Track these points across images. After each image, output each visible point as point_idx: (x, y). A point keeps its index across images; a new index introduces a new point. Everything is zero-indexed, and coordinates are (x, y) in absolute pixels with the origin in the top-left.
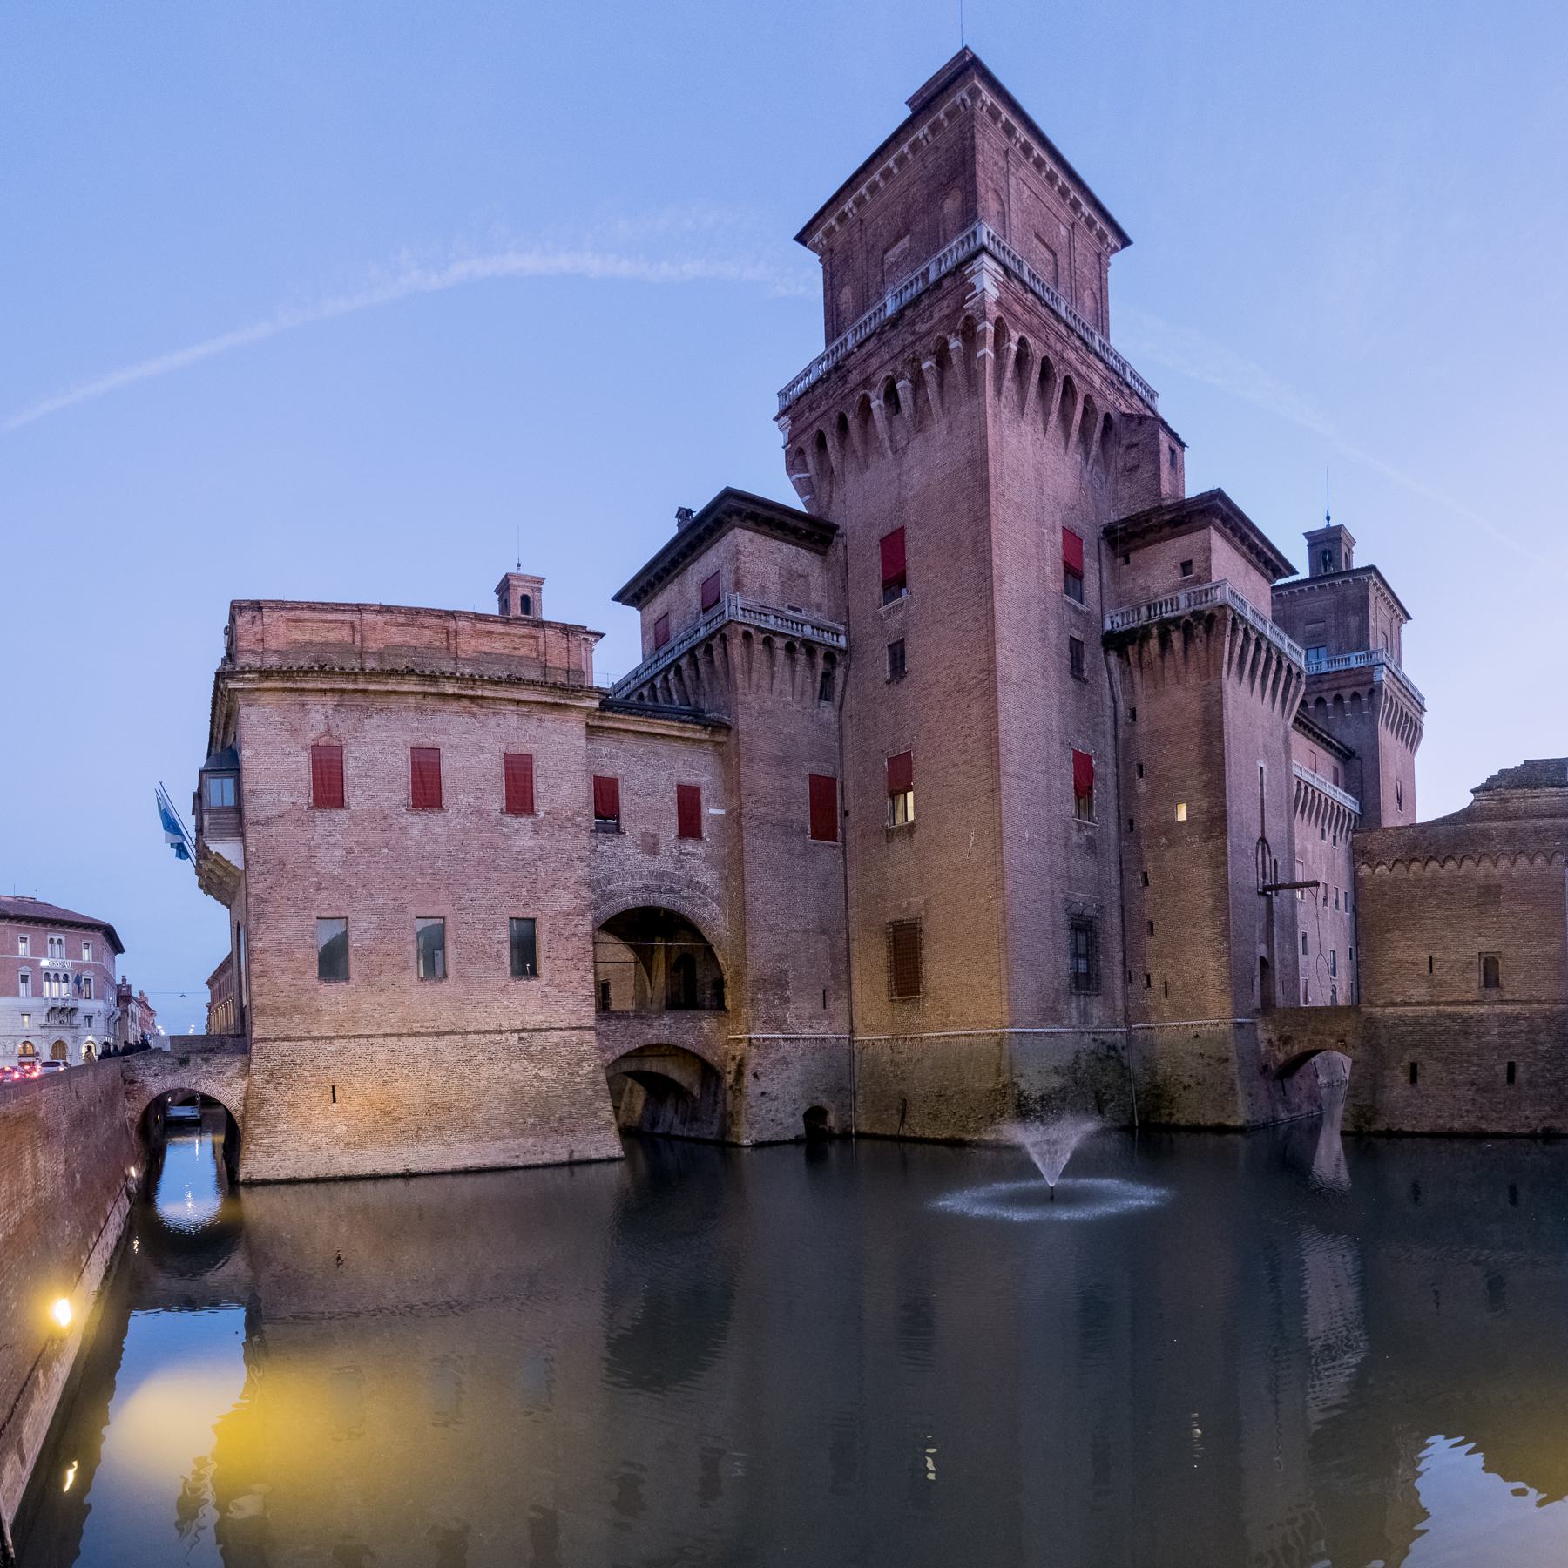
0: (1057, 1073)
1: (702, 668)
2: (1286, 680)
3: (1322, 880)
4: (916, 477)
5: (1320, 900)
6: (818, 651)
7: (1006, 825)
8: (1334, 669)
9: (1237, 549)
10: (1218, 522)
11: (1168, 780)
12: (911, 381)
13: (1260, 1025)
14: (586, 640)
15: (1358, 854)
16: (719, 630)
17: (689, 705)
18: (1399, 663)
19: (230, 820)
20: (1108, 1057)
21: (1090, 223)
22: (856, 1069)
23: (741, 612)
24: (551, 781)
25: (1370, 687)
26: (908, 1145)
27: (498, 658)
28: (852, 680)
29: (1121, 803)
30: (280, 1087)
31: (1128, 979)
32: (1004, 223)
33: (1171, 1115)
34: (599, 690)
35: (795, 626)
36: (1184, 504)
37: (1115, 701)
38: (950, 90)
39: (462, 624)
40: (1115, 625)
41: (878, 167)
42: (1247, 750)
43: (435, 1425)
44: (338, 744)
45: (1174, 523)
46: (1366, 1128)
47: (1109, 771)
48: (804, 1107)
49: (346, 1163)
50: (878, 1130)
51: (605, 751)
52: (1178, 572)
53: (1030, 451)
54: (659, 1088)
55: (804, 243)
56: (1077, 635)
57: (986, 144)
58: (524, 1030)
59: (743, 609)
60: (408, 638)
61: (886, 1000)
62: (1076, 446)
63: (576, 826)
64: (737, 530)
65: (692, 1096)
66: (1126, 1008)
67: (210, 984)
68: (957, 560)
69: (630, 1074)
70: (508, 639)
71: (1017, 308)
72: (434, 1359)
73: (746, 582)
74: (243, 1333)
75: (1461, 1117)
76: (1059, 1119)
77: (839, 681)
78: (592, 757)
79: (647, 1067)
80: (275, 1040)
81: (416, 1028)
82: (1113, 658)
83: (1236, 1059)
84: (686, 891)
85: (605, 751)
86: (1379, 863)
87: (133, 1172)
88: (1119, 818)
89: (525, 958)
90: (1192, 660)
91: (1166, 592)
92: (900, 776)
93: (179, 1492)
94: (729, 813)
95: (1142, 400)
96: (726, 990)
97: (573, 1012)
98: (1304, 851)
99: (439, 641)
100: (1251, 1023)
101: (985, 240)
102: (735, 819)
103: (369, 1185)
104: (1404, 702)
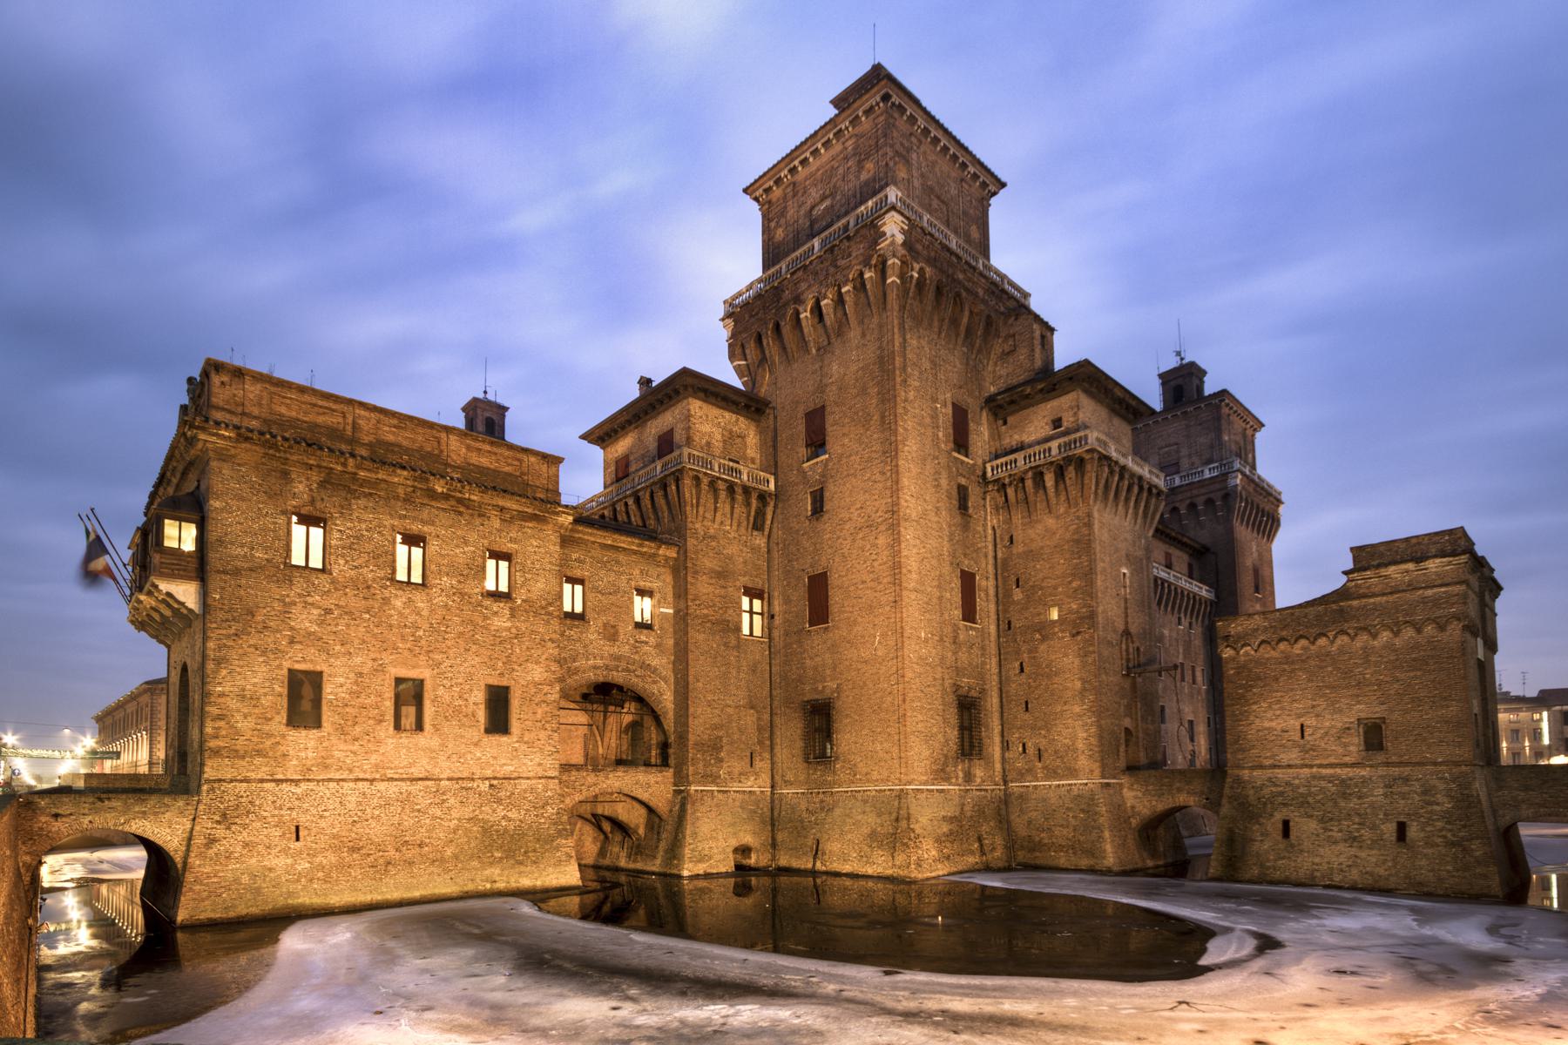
7: (907, 628)
29: (1000, 608)
51: (574, 556)
56: (963, 481)
77: (769, 516)
80: (232, 781)
85: (574, 556)
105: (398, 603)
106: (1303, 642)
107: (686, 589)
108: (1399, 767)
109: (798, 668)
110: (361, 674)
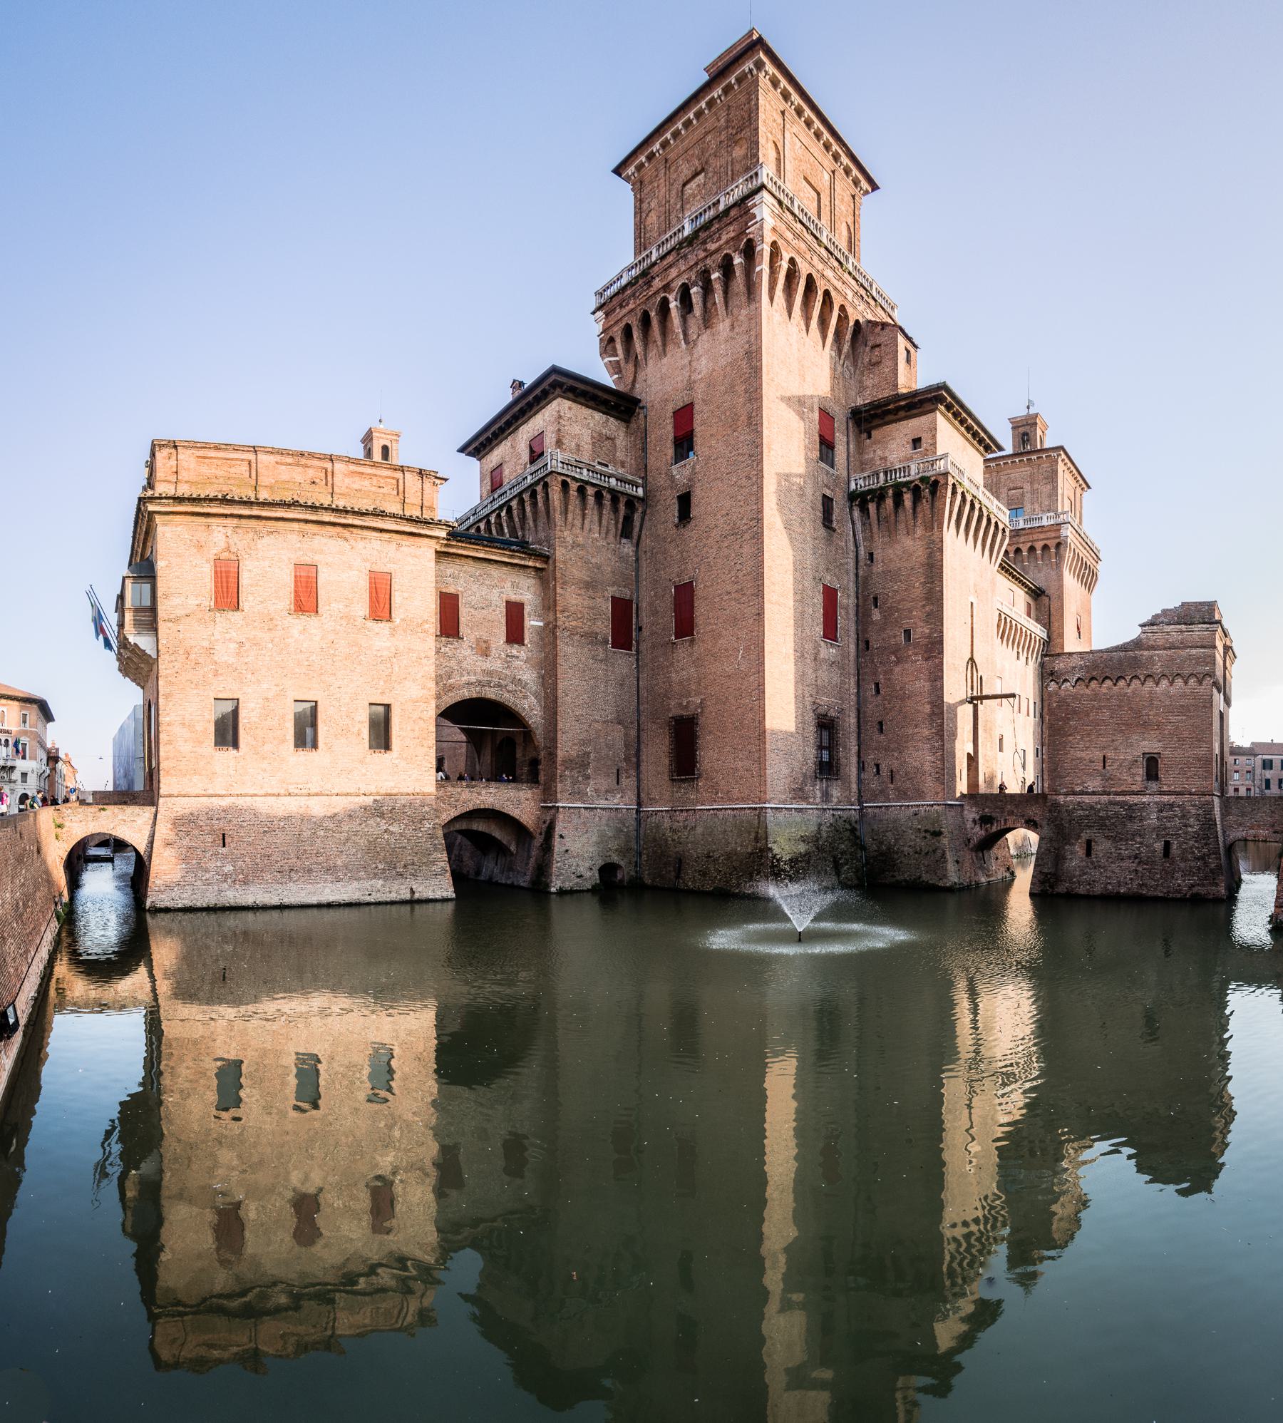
0: (804, 841)
1: (528, 509)
3: (1017, 692)
4: (704, 365)
6: (621, 499)
8: (1029, 526)
12: (701, 287)
13: (966, 807)
15: (1046, 674)
17: (517, 537)
18: (1081, 523)
19: (146, 618)
23: (560, 465)
24: (406, 595)
25: (1057, 541)
28: (647, 524)
31: (861, 767)
32: (780, 167)
35: (603, 478)
37: (857, 546)
38: (740, 61)
40: (859, 486)
44: (236, 558)
45: (909, 407)
48: (600, 863)
49: (233, 896)
51: (449, 572)
52: (909, 446)
54: (483, 843)
55: (620, 175)
56: (828, 493)
57: (767, 105)
59: (563, 463)
61: (667, 778)
63: (425, 631)
64: (559, 400)
65: (510, 851)
66: (859, 791)
69: (460, 832)
70: (375, 479)
71: (789, 236)
73: (565, 441)
75: (1126, 884)
77: (637, 523)
78: (439, 577)
85: (449, 572)
88: (858, 640)
89: (381, 734)
90: (920, 515)
91: (900, 461)
94: (547, 625)
100: (959, 805)
104: (1083, 553)
106: (1108, 682)
107: (555, 601)
108: (1168, 795)
109: (664, 682)
110: (267, 699)
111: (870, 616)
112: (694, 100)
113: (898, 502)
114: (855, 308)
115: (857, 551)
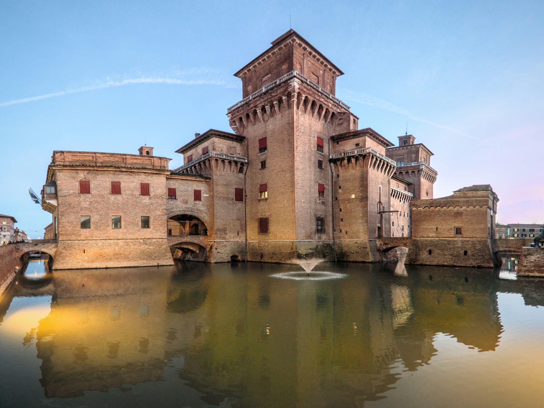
2: (389, 169)
5: (399, 215)
9: (375, 141)
10: (369, 135)
11: (349, 189)
14: (167, 160)
15: (411, 205)
16: (208, 159)
20: (327, 246)
21: (330, 70)
22: (247, 248)
23: (214, 155)
26: (263, 264)
27: (139, 164)
30: (67, 250)
31: (334, 230)
32: (302, 71)
33: (347, 259)
34: (170, 170)
36: (357, 131)
39: (127, 157)
41: (261, 59)
42: (375, 183)
43: (111, 320)
46: (413, 263)
47: (330, 187)
48: (231, 255)
49: (87, 265)
50: (254, 260)
53: (307, 121)
54: (186, 251)
55: (237, 76)
57: (297, 52)
58: (145, 239)
60: (110, 159)
62: (323, 119)
64: (214, 138)
66: (333, 237)
67: (45, 229)
68: (283, 144)
71: (305, 90)
72: (113, 306)
74: (51, 301)
76: (311, 259)
79: (183, 246)
80: (66, 240)
81: (111, 238)
82: (332, 164)
83: (369, 248)
84: (196, 211)
86: (419, 207)
87: (17, 268)
91: (350, 150)
92: (263, 188)
93: (25, 336)
94: (210, 196)
95: (345, 109)
96: (208, 231)
97: (160, 235)
98: (394, 205)
99: (120, 160)
101: (295, 74)
102: (212, 197)
103: (94, 270)
105: (112, 199)
111: (338, 191)
112: (266, 53)
113: (349, 160)
114: (333, 109)
115: (332, 175)
